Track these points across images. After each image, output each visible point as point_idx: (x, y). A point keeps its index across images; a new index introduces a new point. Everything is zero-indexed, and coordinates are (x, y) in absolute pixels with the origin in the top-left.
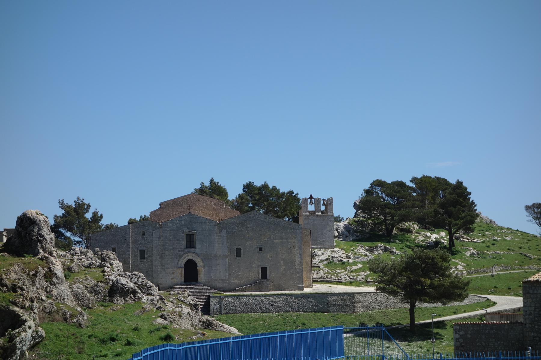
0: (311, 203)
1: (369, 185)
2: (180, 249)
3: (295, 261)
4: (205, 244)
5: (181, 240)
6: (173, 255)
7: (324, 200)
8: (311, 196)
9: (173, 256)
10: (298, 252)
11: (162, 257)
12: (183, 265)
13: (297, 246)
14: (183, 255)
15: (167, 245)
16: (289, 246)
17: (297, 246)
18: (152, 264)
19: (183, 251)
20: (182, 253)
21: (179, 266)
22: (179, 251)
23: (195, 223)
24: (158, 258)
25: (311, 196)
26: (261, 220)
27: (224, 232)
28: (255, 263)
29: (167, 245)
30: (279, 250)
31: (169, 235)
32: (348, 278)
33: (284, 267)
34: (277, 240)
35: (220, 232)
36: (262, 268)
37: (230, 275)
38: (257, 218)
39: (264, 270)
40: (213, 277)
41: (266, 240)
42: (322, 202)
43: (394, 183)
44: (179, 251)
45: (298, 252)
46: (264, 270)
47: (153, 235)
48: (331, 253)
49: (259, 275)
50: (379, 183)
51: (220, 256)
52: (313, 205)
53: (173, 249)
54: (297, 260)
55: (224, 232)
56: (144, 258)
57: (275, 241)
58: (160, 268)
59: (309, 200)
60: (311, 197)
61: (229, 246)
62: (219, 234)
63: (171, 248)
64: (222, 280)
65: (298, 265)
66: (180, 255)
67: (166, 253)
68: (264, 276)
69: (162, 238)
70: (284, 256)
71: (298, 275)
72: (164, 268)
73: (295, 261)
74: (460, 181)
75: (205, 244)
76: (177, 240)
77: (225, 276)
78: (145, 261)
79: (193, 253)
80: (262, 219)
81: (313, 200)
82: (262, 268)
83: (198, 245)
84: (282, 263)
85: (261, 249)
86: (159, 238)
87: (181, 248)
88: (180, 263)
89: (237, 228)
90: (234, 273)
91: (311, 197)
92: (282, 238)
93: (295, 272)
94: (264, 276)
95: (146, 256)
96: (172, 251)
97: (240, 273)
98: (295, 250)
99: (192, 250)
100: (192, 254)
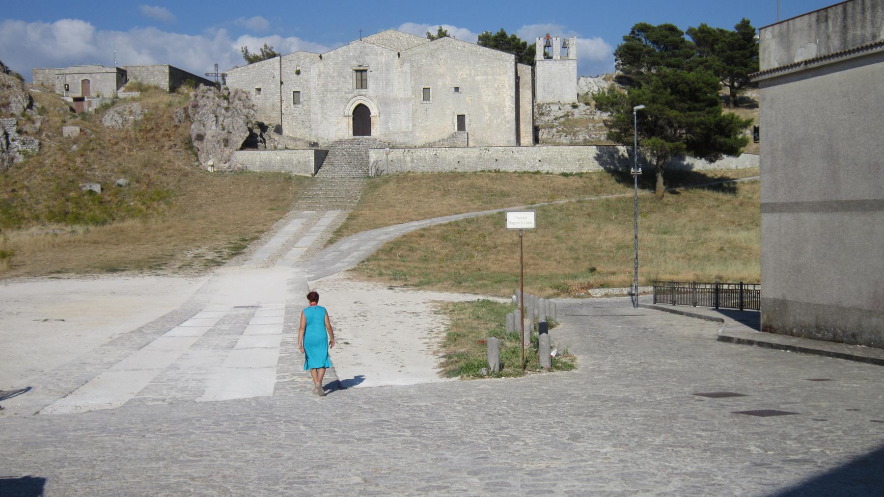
1: (630, 31)
2: (347, 90)
3: (505, 107)
4: (381, 83)
5: (348, 77)
6: (337, 98)
9: (338, 100)
10: (509, 93)
11: (322, 101)
13: (507, 86)
15: (330, 84)
16: (496, 85)
17: (507, 86)
18: (309, 112)
19: (351, 93)
20: (350, 96)
21: (346, 114)
22: (346, 93)
23: (367, 55)
26: (458, 49)
27: (407, 67)
28: (448, 109)
29: (330, 84)
32: (588, 137)
33: (488, 115)
35: (402, 65)
36: (458, 116)
37: (414, 125)
38: (451, 46)
39: (461, 119)
40: (391, 129)
41: (465, 76)
43: (660, 27)
44: (346, 93)
45: (509, 93)
46: (461, 119)
47: (312, 71)
50: (643, 28)
51: (401, 99)
53: (338, 90)
55: (407, 67)
56: (299, 103)
57: (477, 78)
58: (320, 116)
61: (413, 86)
62: (400, 70)
63: (336, 89)
64: (404, 132)
65: (508, 111)
66: (346, 99)
67: (329, 95)
69: (322, 75)
70: (489, 100)
71: (508, 126)
72: (325, 116)
73: (505, 107)
74: (746, 19)
75: (381, 83)
76: (344, 77)
77: (408, 128)
78: (300, 106)
79: (365, 96)
80: (459, 48)
82: (458, 116)
83: (371, 83)
84: (486, 108)
85: (457, 89)
86: (319, 75)
89: (424, 60)
90: (419, 123)
92: (486, 74)
93: (503, 122)
95: (301, 100)
96: (336, 93)
98: (505, 90)
99: (363, 91)
100: (363, 98)
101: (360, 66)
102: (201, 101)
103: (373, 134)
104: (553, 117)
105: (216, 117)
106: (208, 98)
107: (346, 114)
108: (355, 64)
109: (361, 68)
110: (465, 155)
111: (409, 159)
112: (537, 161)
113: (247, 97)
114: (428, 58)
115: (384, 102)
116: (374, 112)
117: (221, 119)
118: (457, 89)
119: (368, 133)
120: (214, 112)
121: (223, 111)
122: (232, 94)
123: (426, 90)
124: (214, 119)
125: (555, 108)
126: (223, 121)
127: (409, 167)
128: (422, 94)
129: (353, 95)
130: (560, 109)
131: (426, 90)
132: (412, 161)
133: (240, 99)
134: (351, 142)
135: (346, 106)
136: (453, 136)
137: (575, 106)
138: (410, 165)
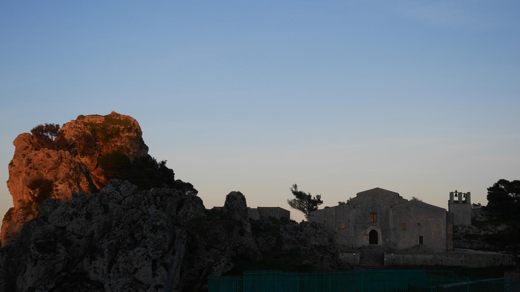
0: (456, 196)
2: (366, 223)
7: (464, 194)
8: (456, 191)
10: (444, 227)
12: (368, 234)
14: (369, 227)
16: (438, 223)
21: (366, 234)
22: (366, 224)
24: (353, 228)
25: (456, 191)
30: (431, 225)
31: (360, 213)
32: (478, 245)
34: (430, 219)
36: (420, 237)
39: (421, 238)
41: (423, 218)
42: (463, 195)
46: (421, 238)
48: (469, 229)
49: (418, 241)
52: (457, 197)
54: (442, 232)
59: (455, 194)
60: (456, 192)
63: (361, 222)
73: (442, 233)
80: (420, 205)
81: (457, 193)
82: (420, 237)
87: (367, 222)
88: (366, 232)
89: (403, 210)
91: (456, 192)
93: (441, 240)
96: (361, 224)
97: (405, 240)
98: (442, 225)
99: (375, 224)
101: (373, 212)
102: (305, 229)
103: (378, 244)
104: (459, 233)
105: (315, 237)
106: (307, 227)
107: (366, 234)
109: (374, 213)
110: (427, 257)
111: (402, 258)
112: (460, 261)
113: (324, 227)
114: (406, 209)
117: (317, 238)
118: (419, 224)
119: (377, 243)
120: (314, 235)
121: (318, 235)
122: (318, 225)
124: (315, 238)
125: (460, 228)
126: (318, 239)
128: (402, 226)
129: (369, 225)
130: (463, 229)
132: (403, 260)
133: (321, 228)
135: (366, 230)
138: (402, 261)
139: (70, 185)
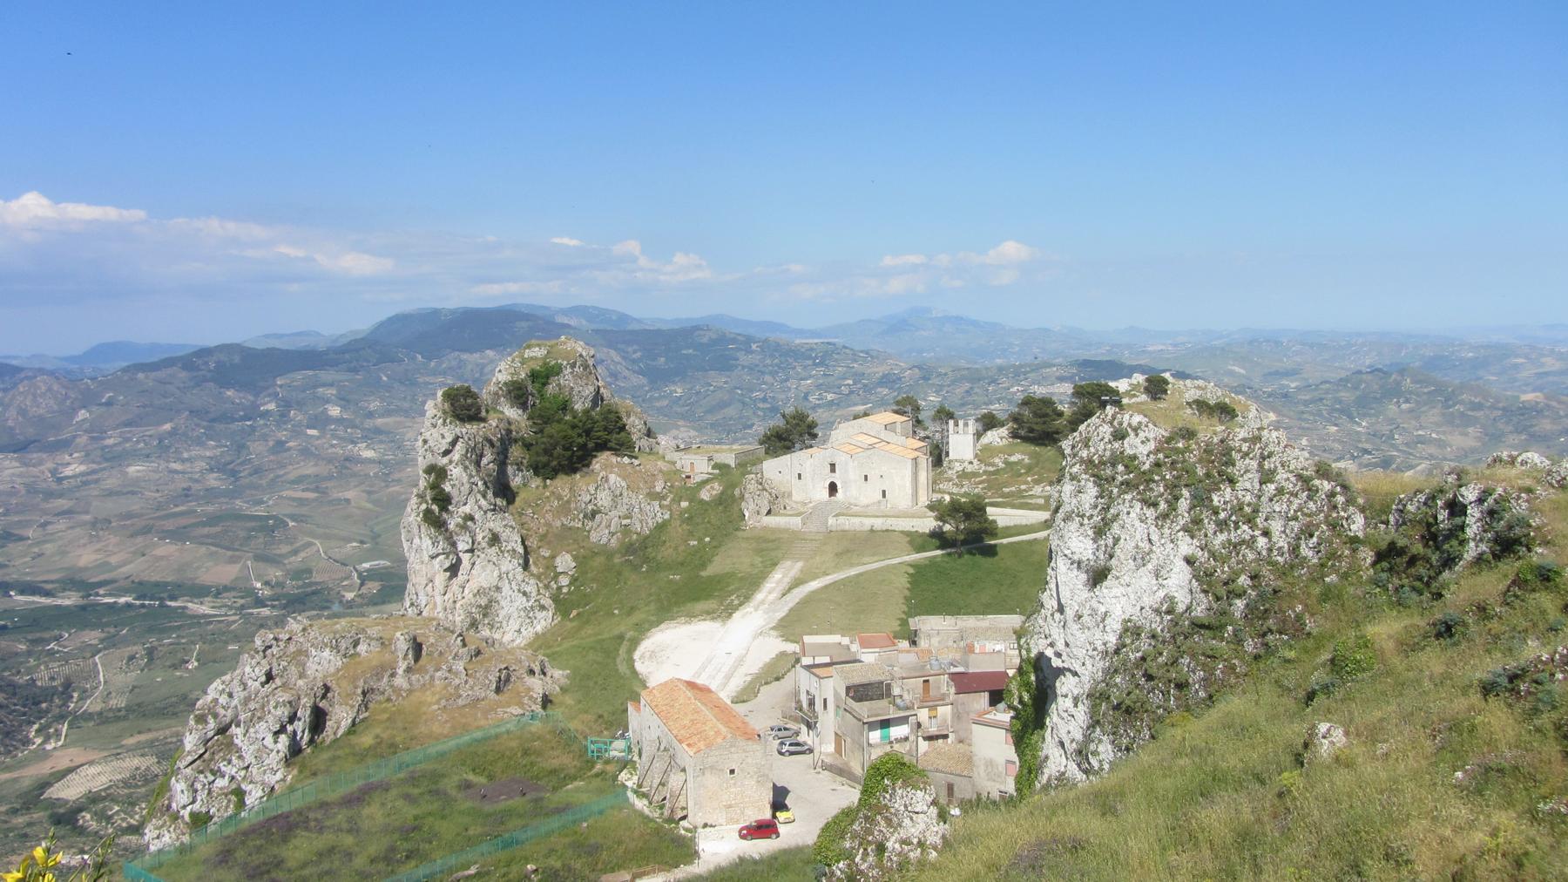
27: (856, 462)
39: (884, 492)
46: (884, 492)
68: (884, 496)
94: (884, 496)
99: (833, 475)
108: (830, 461)
115: (844, 483)
116: (839, 486)
123: (866, 477)
127: (847, 528)
131: (866, 477)
134: (827, 503)
136: (879, 502)
137: (971, 463)
139: (466, 468)
